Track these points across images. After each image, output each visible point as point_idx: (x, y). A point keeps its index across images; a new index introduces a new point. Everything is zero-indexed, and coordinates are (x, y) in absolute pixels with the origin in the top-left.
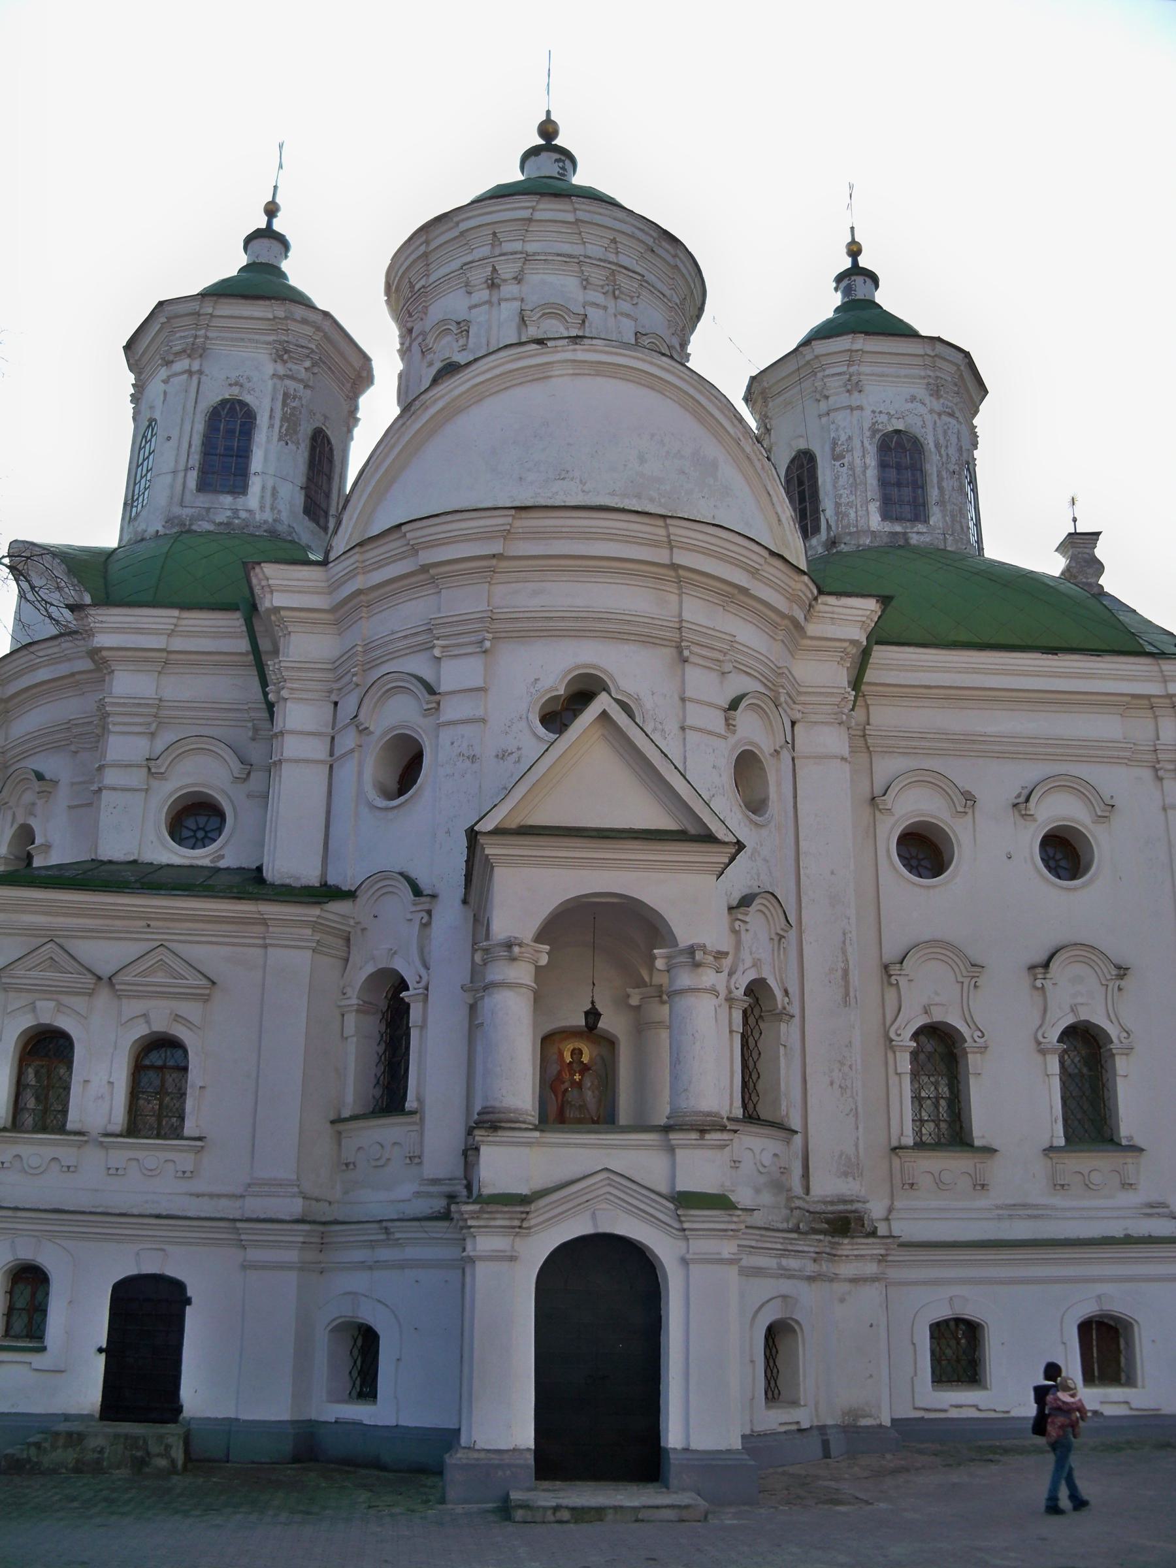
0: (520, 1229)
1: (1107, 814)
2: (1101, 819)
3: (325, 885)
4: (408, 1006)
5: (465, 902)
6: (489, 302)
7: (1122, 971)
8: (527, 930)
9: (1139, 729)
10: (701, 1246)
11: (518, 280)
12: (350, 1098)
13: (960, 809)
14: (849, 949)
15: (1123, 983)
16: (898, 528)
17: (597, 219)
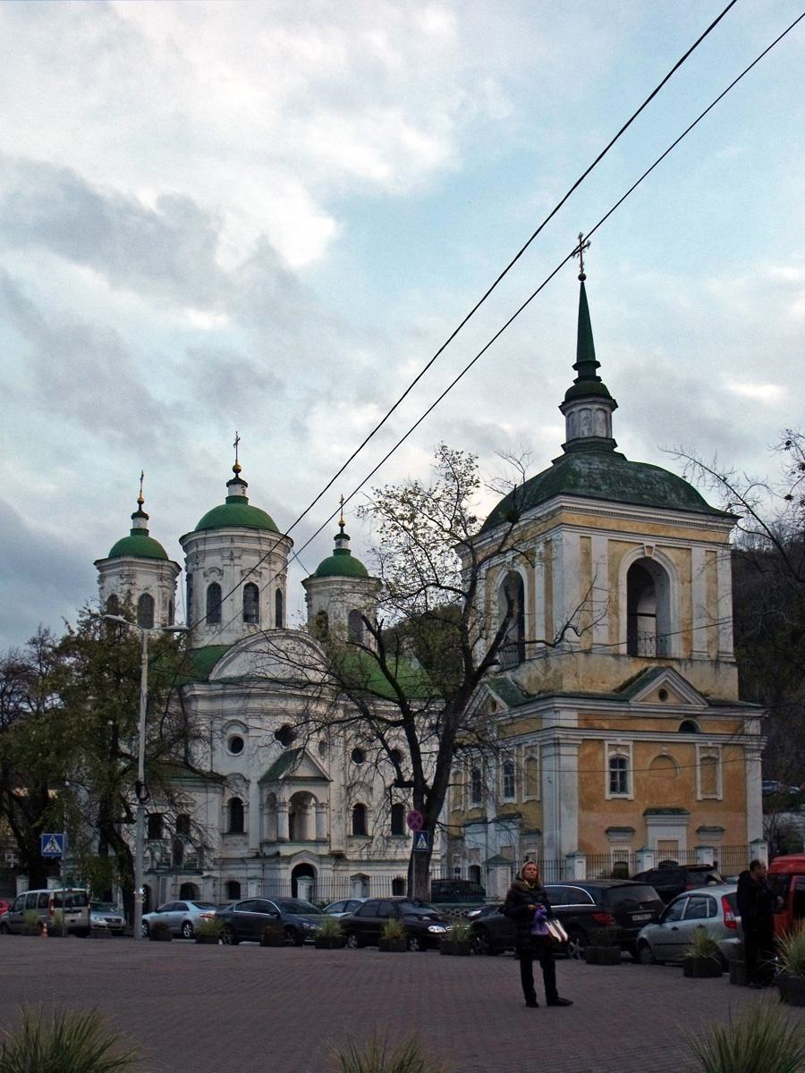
0: (289, 863)
3: (211, 771)
4: (242, 807)
5: (258, 783)
6: (230, 565)
8: (287, 800)
10: (324, 866)
11: (239, 558)
12: (226, 829)
17: (267, 536)
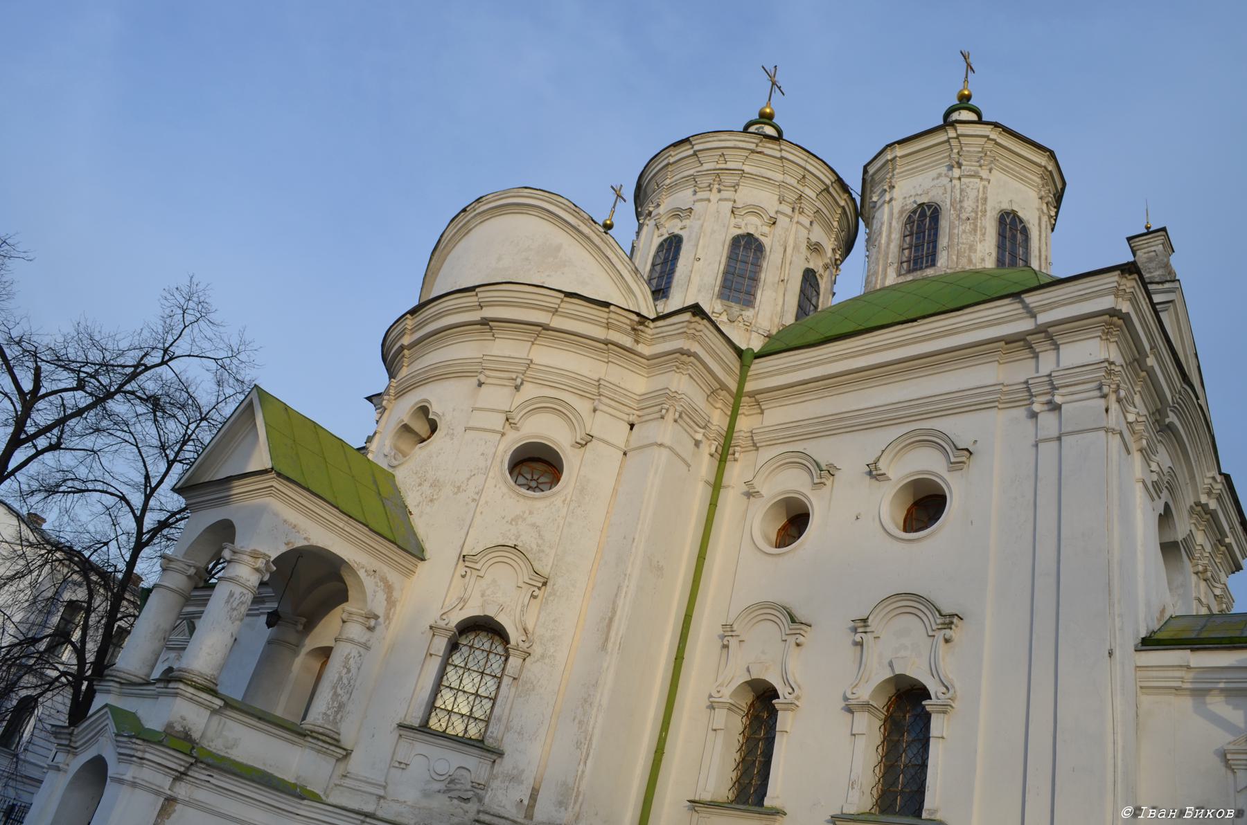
1: (964, 459)
2: (955, 466)
7: (949, 620)
9: (1018, 371)
13: (816, 481)
14: (620, 602)
15: (948, 633)
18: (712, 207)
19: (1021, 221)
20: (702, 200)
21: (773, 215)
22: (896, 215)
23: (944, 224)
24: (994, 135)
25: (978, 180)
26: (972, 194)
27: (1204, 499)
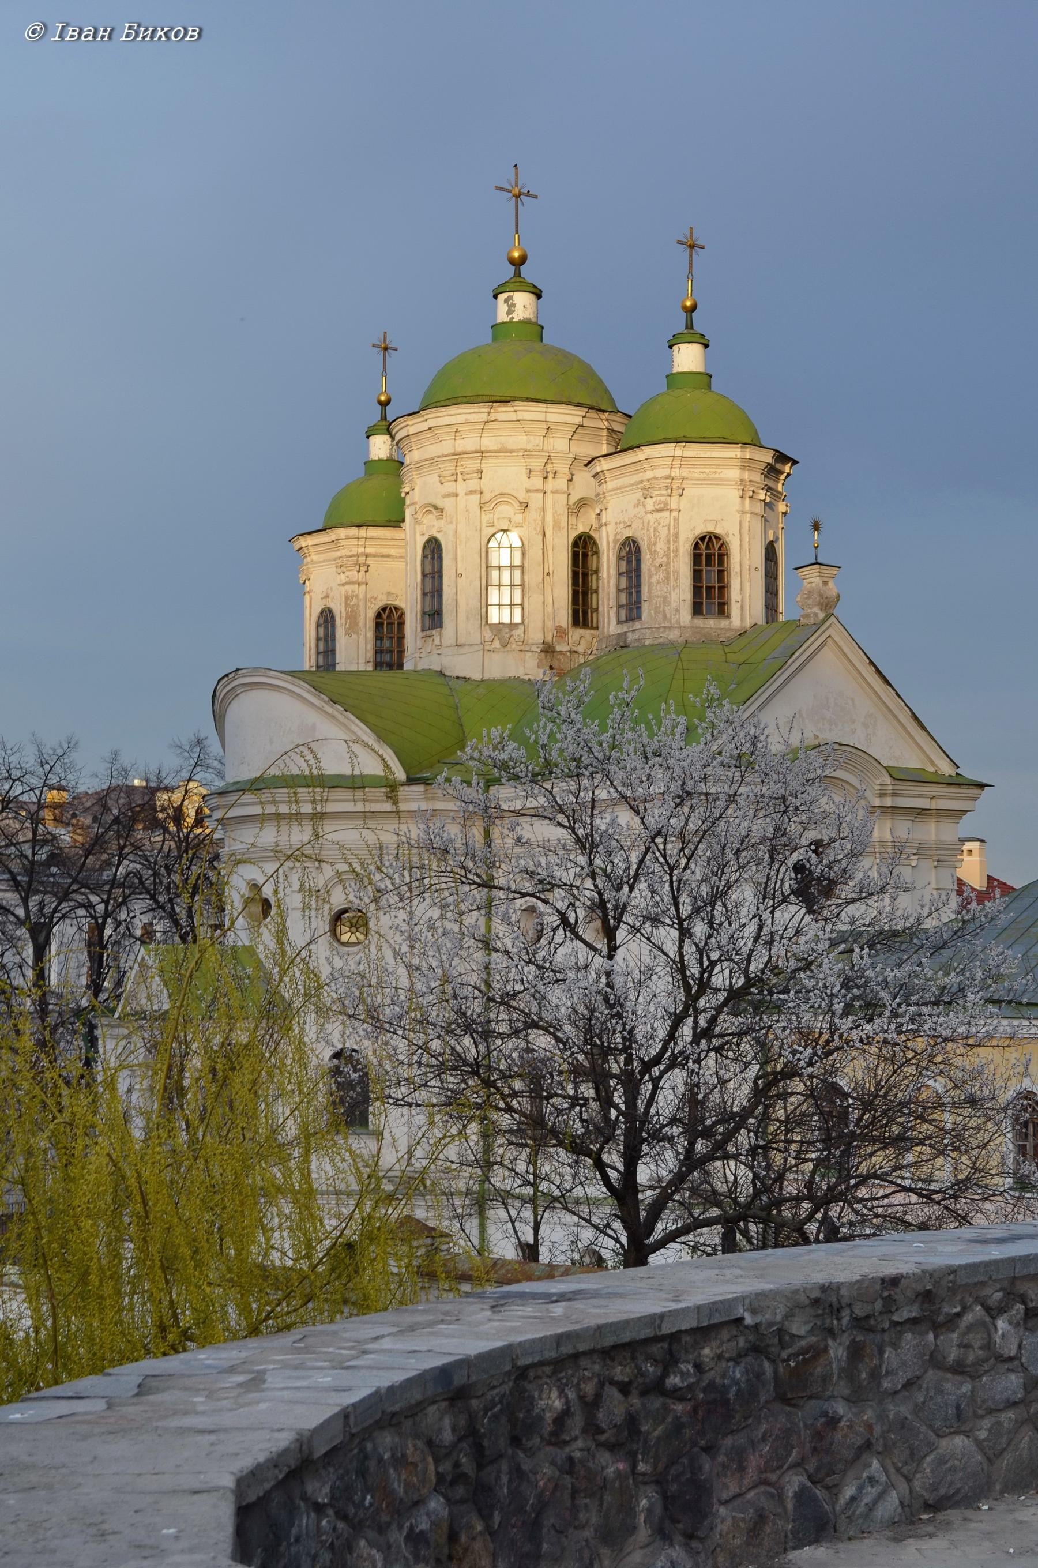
16: (624, 628)
18: (462, 500)
19: (718, 538)
20: (449, 495)
21: (522, 496)
22: (611, 545)
23: (644, 567)
24: (678, 450)
25: (666, 514)
26: (663, 532)
27: (877, 802)
